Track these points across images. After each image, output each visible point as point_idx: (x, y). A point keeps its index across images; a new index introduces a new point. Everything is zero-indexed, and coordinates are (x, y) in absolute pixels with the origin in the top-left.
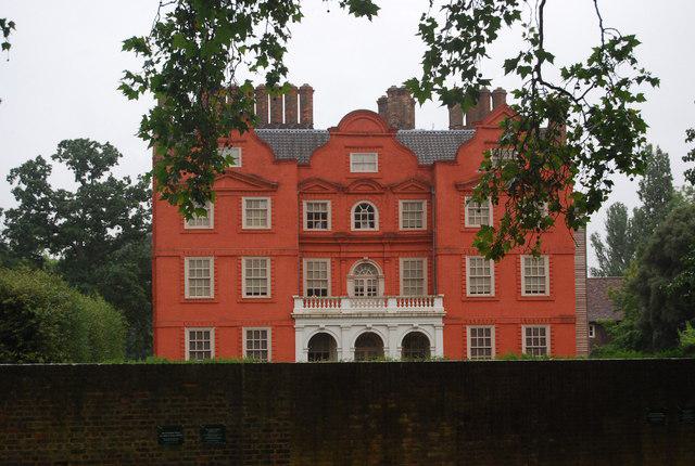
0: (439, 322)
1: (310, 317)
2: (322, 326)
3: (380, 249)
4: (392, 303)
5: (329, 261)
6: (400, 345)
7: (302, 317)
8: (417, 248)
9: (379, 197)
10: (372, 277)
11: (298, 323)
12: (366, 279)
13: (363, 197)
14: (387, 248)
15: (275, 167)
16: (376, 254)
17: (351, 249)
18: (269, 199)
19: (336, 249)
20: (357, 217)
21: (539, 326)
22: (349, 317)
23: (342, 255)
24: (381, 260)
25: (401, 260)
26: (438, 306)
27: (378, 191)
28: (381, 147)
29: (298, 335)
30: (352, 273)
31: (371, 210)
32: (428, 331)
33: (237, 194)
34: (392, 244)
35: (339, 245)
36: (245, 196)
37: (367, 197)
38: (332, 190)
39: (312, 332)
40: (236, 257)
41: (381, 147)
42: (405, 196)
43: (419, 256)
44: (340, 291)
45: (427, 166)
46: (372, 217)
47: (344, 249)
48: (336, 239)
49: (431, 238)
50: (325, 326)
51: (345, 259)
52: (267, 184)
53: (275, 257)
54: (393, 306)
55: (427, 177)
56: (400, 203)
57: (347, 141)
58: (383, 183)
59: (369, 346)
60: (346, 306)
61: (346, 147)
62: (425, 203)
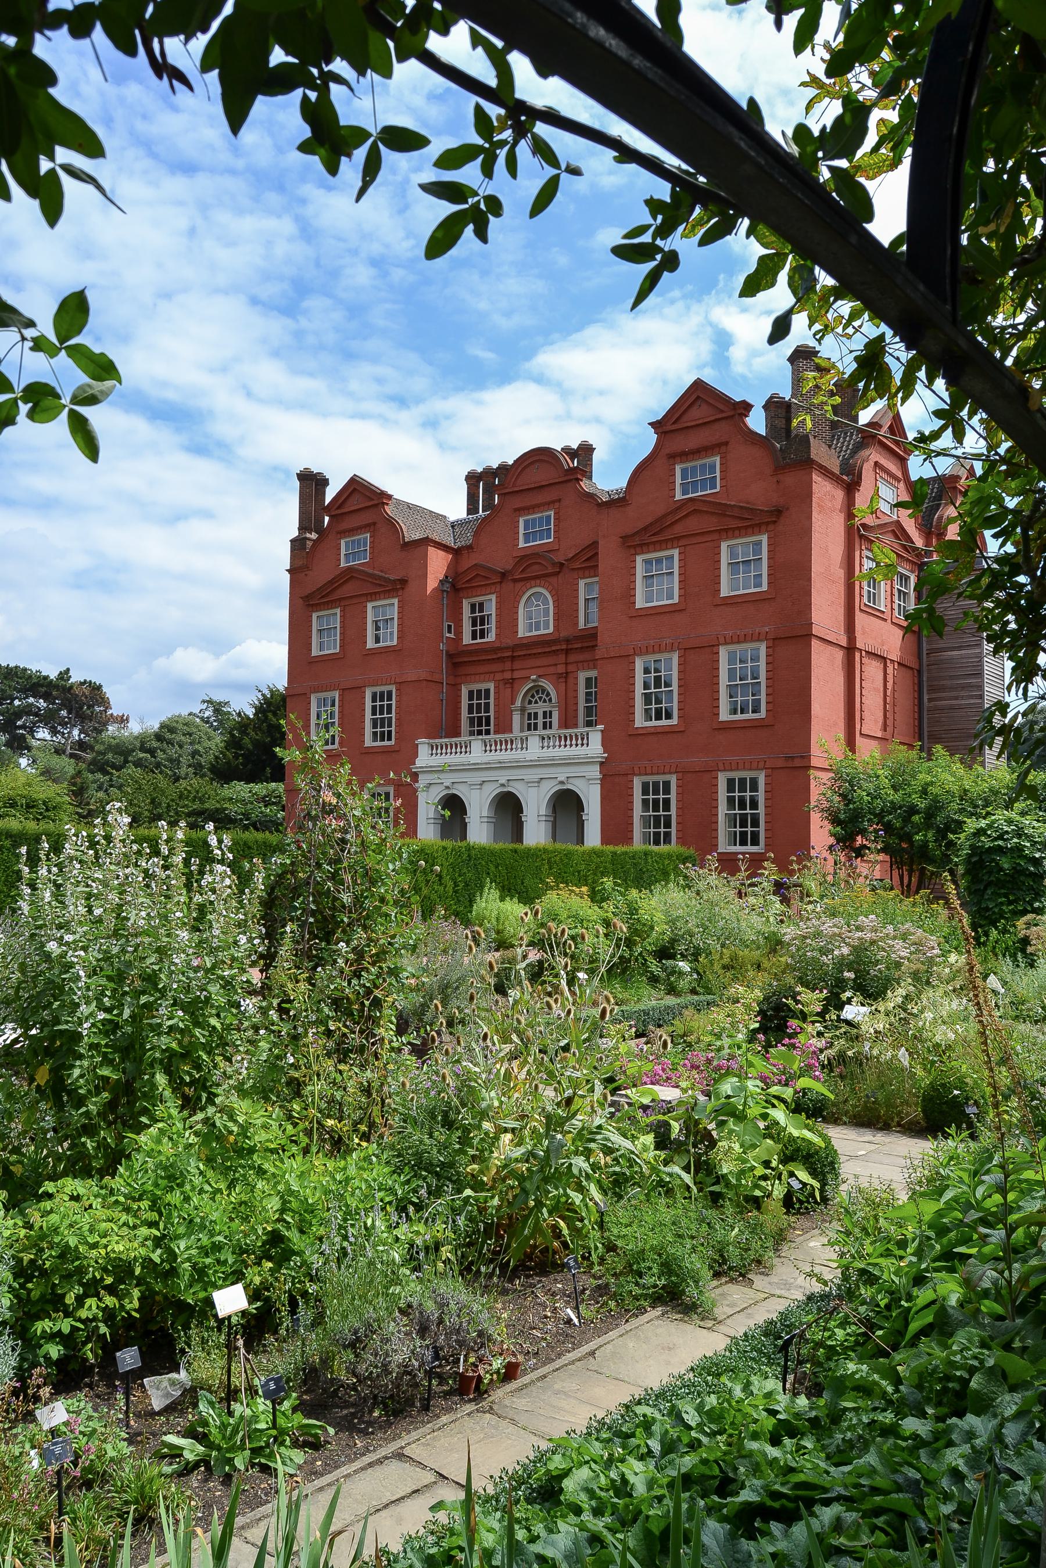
0: (595, 772)
1: (440, 771)
3: (551, 660)
4: (534, 742)
7: (430, 770)
9: (553, 580)
11: (423, 781)
16: (552, 670)
17: (517, 664)
21: (747, 775)
22: (488, 768)
23: (508, 675)
26: (595, 746)
27: (550, 570)
28: (559, 500)
29: (422, 798)
30: (518, 703)
31: (545, 602)
32: (578, 786)
57: (518, 502)
58: (560, 558)
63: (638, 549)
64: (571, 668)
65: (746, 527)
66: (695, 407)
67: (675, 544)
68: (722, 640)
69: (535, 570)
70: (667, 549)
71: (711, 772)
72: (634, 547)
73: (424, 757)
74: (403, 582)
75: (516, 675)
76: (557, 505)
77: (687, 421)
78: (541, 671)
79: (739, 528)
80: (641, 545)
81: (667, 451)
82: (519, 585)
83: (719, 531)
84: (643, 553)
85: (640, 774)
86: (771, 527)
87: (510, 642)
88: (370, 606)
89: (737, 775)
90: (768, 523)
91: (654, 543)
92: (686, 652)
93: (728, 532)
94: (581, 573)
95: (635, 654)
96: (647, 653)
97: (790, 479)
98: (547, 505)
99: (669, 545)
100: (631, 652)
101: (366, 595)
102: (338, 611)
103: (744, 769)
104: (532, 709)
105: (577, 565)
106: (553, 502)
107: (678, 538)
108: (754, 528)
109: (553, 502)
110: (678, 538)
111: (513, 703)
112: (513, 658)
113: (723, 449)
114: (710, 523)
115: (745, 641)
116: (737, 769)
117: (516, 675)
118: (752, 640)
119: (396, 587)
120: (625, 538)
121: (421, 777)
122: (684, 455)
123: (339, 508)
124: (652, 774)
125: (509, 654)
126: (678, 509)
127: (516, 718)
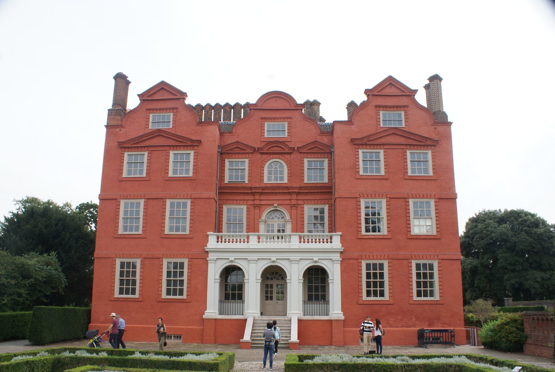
0: (337, 257)
2: (232, 259)
3: (288, 197)
4: (295, 239)
5: (245, 207)
6: (301, 277)
8: (318, 197)
9: (287, 156)
10: (281, 221)
11: (211, 256)
12: (276, 223)
13: (275, 156)
14: (294, 197)
15: (199, 127)
17: (263, 197)
18: (192, 153)
19: (251, 197)
20: (270, 173)
23: (257, 202)
24: (289, 206)
25: (306, 207)
26: (337, 243)
28: (291, 118)
30: (263, 217)
31: (281, 166)
32: (325, 265)
33: (168, 148)
34: (298, 194)
35: (253, 194)
36: (174, 150)
37: (278, 156)
38: (249, 151)
39: (222, 265)
40: (163, 200)
41: (291, 118)
42: (309, 155)
43: (321, 204)
44: (253, 227)
45: (328, 132)
46: (282, 172)
47: (257, 197)
48: (251, 188)
49: (331, 188)
50: (232, 259)
51: (259, 206)
52: (191, 140)
53: (194, 200)
54: (294, 242)
55: (325, 140)
56: (306, 160)
58: (291, 145)
59: (278, 279)
60: (253, 243)
61: (262, 118)
62: (326, 161)
63: (360, 146)
64: (300, 202)
65: (421, 146)
66: (388, 88)
67: (382, 147)
68: (411, 196)
69: (276, 149)
70: (377, 149)
71: (408, 260)
72: (358, 145)
73: (212, 243)
74: (200, 142)
75: (263, 202)
76: (289, 120)
77: (384, 92)
78: (280, 202)
79: (417, 145)
80: (362, 145)
81: (374, 104)
82: (265, 156)
83: (406, 145)
84: (363, 149)
85: (366, 259)
86: (433, 148)
87: (257, 185)
88: (172, 153)
89: (421, 262)
90: (432, 146)
91: (370, 145)
92: (390, 199)
93: (410, 146)
94: (305, 155)
95: (360, 197)
96: (368, 197)
97: (440, 128)
98: (284, 119)
99: (378, 147)
100: (358, 196)
101: (170, 146)
102: (146, 153)
103: (427, 259)
104: (270, 222)
105: (304, 151)
106: (288, 118)
107: (384, 145)
108: (426, 146)
109: (288, 118)
110: (384, 145)
111: (260, 218)
112: (262, 193)
113: (406, 109)
114: (402, 141)
115: (423, 198)
116: (423, 259)
117: (263, 202)
118: (427, 198)
119: (194, 144)
120: (352, 140)
121: (210, 254)
122: (385, 107)
123: (149, 96)
124: (373, 259)
125: (261, 191)
126: (385, 131)
127: (262, 227)
